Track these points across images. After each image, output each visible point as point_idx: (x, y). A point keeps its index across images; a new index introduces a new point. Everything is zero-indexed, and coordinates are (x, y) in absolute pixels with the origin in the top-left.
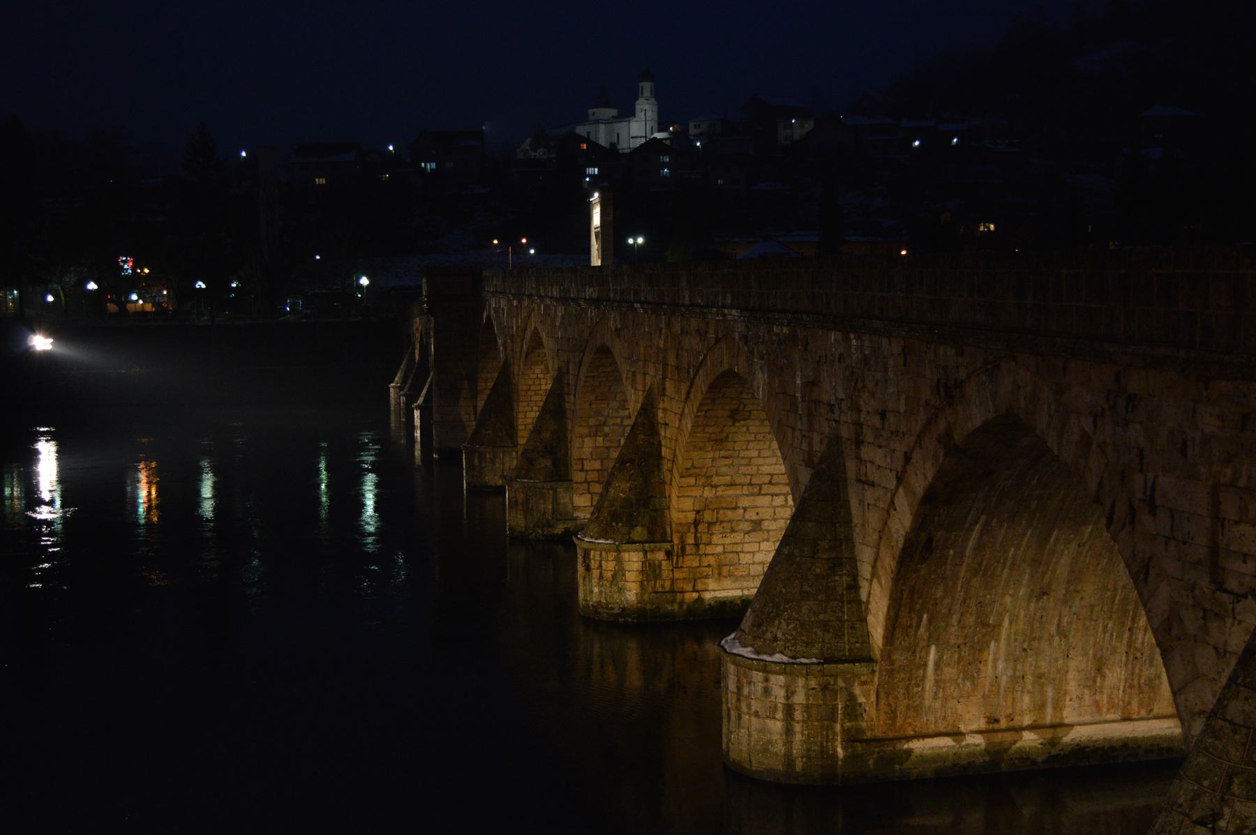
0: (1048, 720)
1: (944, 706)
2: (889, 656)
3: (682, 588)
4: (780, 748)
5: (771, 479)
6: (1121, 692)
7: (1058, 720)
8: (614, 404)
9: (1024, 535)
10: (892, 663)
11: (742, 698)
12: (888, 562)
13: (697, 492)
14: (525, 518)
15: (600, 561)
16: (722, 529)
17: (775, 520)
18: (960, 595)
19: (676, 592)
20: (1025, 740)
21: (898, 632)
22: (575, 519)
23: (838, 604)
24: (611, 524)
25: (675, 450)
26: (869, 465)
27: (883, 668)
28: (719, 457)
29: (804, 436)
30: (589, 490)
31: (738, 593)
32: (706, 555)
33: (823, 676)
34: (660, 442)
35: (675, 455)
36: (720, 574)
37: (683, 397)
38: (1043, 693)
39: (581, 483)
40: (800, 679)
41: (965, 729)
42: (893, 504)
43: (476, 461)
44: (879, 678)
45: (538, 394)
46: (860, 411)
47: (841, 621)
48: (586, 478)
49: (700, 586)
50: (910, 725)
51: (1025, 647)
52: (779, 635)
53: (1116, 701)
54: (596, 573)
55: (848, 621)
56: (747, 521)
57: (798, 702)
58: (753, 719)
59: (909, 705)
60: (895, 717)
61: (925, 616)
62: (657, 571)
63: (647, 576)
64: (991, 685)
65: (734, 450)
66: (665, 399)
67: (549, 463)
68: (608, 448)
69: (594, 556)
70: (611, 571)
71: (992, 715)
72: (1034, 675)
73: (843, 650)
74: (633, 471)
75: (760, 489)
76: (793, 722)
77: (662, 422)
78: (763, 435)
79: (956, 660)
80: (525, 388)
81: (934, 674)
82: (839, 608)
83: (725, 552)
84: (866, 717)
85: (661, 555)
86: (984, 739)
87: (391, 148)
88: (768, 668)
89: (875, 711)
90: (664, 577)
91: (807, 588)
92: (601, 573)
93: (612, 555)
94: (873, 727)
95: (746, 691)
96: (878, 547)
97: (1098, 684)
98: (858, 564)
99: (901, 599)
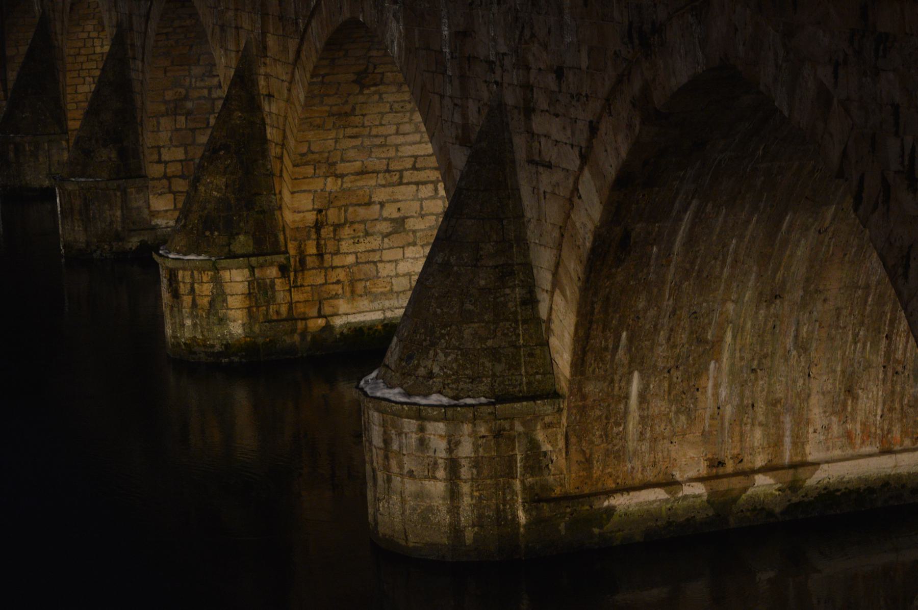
0: (787, 457)
1: (652, 449)
2: (580, 389)
3: (304, 313)
4: (444, 518)
5: (415, 162)
6: (878, 418)
7: (798, 459)
8: (196, 71)
9: (748, 222)
10: (584, 397)
11: (390, 454)
12: (573, 267)
13: (318, 184)
14: (86, 230)
15: (192, 285)
16: (352, 232)
17: (422, 216)
18: (668, 303)
19: (296, 320)
20: (758, 486)
21: (590, 358)
22: (154, 228)
23: (511, 325)
24: (204, 233)
25: (284, 130)
26: (543, 140)
27: (572, 405)
28: (344, 137)
29: (456, 105)
30: (170, 187)
31: (377, 316)
32: (333, 268)
33: (496, 419)
34: (263, 120)
35: (285, 137)
36: (353, 292)
37: (292, 56)
38: (778, 422)
39: (159, 179)
40: (465, 426)
41: (681, 477)
42: (578, 190)
43: (12, 155)
44: (567, 418)
45: (92, 60)
46: (528, 69)
47: (515, 346)
48: (165, 173)
49: (327, 310)
50: (610, 476)
51: (754, 367)
52: (436, 370)
53: (873, 430)
54: (187, 300)
55: (524, 346)
56: (385, 219)
57: (464, 456)
58: (406, 480)
59: (608, 450)
60: (591, 468)
61: (624, 334)
62: (270, 293)
63: (257, 300)
64: (712, 418)
65: (363, 126)
66: (268, 61)
67: (114, 155)
68: (193, 130)
70: (208, 296)
71: (715, 457)
72: (766, 403)
73: (520, 385)
75: (401, 177)
76: (458, 482)
77: (265, 93)
78: (402, 104)
79: (666, 389)
80: (72, 52)
81: (639, 409)
82: (512, 330)
83: (357, 263)
85: (273, 272)
86: (706, 489)
88: (424, 413)
89: (564, 461)
90: (279, 300)
91: (469, 306)
92: (194, 300)
95: (395, 446)
96: (559, 247)
97: (849, 409)
98: (535, 271)
99: (592, 313)
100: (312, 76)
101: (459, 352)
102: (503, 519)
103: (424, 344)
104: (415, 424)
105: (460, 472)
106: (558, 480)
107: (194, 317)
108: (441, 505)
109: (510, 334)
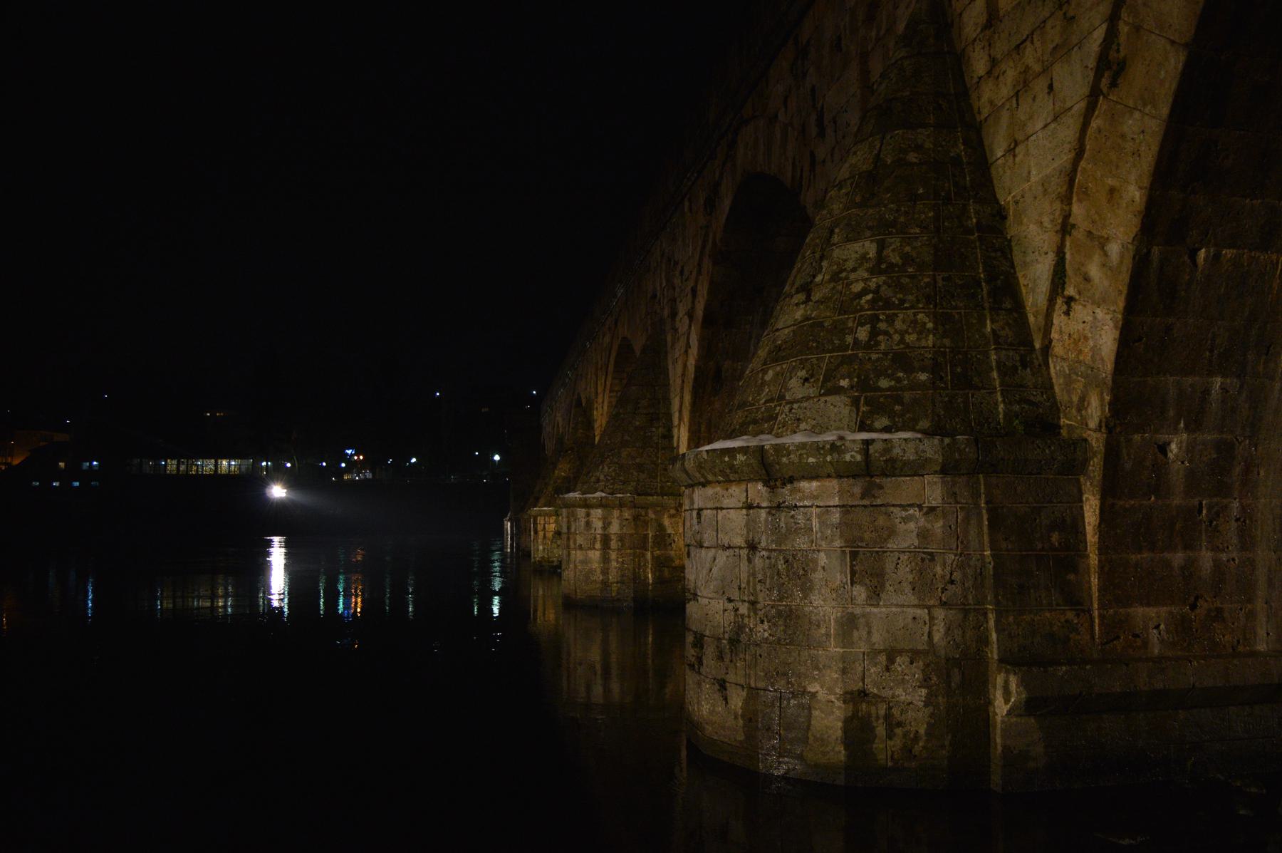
12: (688, 398)
33: (635, 507)
40: (615, 511)
52: (602, 477)
54: (541, 534)
55: (661, 464)
58: (578, 552)
87: (534, 392)
91: (627, 437)
92: (545, 535)
93: (552, 519)
95: (573, 530)
100: (610, 392)
102: (637, 579)
107: (544, 544)
108: (595, 565)
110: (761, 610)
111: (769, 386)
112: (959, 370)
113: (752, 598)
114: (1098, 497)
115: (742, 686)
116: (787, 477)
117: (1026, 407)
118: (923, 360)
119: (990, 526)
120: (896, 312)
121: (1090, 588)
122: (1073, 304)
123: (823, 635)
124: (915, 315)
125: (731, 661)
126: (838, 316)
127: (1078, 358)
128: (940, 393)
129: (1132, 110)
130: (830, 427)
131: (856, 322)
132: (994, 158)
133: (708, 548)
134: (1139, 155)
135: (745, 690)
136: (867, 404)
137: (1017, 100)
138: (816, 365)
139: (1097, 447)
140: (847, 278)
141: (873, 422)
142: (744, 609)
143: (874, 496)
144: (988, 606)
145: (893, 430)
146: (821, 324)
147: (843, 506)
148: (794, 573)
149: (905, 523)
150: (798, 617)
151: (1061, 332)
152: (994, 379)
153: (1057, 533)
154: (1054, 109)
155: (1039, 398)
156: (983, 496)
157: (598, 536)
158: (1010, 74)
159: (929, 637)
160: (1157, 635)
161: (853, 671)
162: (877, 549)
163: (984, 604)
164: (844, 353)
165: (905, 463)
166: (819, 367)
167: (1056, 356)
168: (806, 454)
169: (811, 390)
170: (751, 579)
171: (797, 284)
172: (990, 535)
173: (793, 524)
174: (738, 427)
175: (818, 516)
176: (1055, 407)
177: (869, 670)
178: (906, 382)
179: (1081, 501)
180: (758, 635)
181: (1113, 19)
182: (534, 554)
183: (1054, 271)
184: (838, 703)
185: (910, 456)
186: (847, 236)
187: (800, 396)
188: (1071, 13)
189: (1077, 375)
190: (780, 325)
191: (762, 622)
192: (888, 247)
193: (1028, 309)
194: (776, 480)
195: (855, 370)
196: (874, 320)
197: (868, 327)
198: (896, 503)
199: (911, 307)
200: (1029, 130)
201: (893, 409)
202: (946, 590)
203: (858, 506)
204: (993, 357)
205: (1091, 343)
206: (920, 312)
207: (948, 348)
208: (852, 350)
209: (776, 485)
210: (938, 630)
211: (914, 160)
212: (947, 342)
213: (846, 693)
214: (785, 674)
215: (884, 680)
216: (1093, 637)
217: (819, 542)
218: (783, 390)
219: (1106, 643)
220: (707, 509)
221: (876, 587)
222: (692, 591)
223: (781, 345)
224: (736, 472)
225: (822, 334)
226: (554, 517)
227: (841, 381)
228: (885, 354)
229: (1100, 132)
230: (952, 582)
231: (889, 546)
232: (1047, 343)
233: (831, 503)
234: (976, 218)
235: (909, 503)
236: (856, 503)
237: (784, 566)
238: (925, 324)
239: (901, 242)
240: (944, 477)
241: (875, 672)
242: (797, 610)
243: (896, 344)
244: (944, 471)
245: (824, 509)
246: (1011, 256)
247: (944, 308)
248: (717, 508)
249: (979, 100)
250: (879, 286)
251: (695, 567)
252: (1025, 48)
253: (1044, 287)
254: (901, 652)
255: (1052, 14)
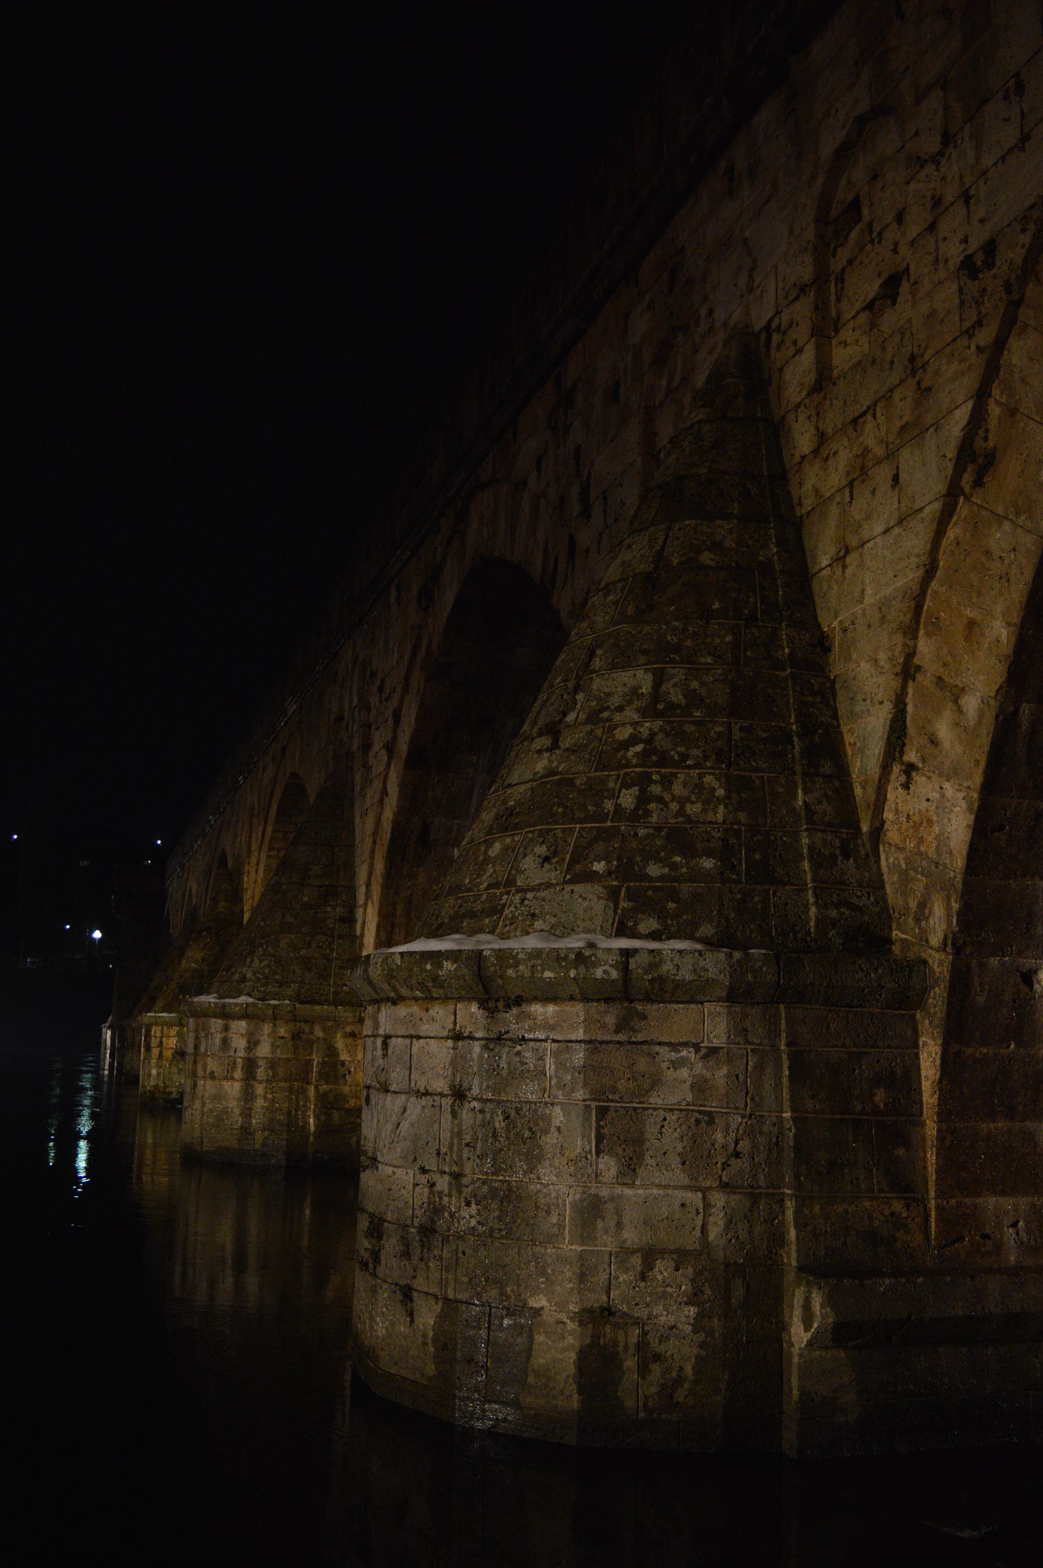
4: (237, 1120)
12: (380, 866)
15: (161, 1038)
23: (327, 940)
33: (295, 1020)
34: (243, 909)
40: (266, 1025)
47: (327, 959)
52: (249, 975)
54: (155, 1051)
58: (208, 1082)
69: (155, 1032)
70: (172, 1048)
73: (327, 994)
74: (209, 940)
82: (327, 943)
84: (350, 1080)
91: (289, 919)
92: (161, 1052)
93: (174, 1031)
94: (358, 1094)
95: (202, 1049)
100: (269, 850)
101: (273, 959)
103: (244, 953)
104: (220, 1023)
105: (256, 1072)
106: (354, 1091)
107: (159, 1067)
108: (233, 1105)
109: (325, 947)
110: (467, 1187)
111: (494, 865)
112: (757, 857)
113: (455, 1169)
114: (939, 1042)
115: (436, 1297)
116: (513, 997)
117: (847, 912)
118: (708, 840)
119: (792, 1076)
120: (675, 771)
121: (925, 1168)
122: (914, 774)
123: (554, 1225)
124: (701, 776)
125: (422, 1260)
126: (595, 771)
127: (918, 848)
128: (730, 887)
129: (1001, 518)
130: (576, 929)
131: (620, 781)
132: (817, 568)
133: (395, 1092)
134: (1008, 581)
135: (440, 1303)
136: (629, 897)
137: (851, 492)
138: (561, 838)
139: (940, 973)
140: (609, 719)
141: (636, 924)
142: (443, 1183)
143: (634, 1030)
144: (786, 1190)
145: (664, 937)
146: (570, 782)
147: (590, 1042)
148: (516, 1135)
149: (675, 1069)
150: (519, 1198)
151: (897, 812)
152: (805, 871)
153: (882, 1090)
154: (899, 509)
155: (864, 900)
156: (784, 1035)
157: (239, 1060)
158: (844, 457)
159: (702, 1232)
160: (1014, 1236)
161: (594, 1279)
162: (634, 1105)
163: (779, 1188)
164: (603, 825)
165: (678, 985)
166: (566, 842)
167: (890, 844)
168: (541, 965)
169: (553, 875)
170: (455, 1141)
171: (541, 723)
172: (792, 1090)
173: (518, 1065)
174: (447, 920)
175: (555, 1054)
176: (885, 914)
177: (617, 1278)
178: (684, 870)
179: (917, 1046)
180: (462, 1222)
181: (981, 396)
182: (143, 1081)
183: (891, 727)
184: (571, 1326)
185: (686, 974)
186: (613, 661)
187: (537, 882)
188: (926, 383)
189: (916, 871)
190: (514, 779)
191: (468, 1204)
192: (668, 680)
193: (854, 776)
194: (497, 1001)
195: (615, 849)
196: (644, 780)
197: (635, 790)
198: (663, 1040)
199: (697, 766)
200: (865, 534)
201: (665, 907)
202: (729, 1165)
203: (610, 1042)
204: (805, 841)
205: (936, 829)
206: (708, 773)
207: (745, 825)
208: (612, 821)
209: (497, 1007)
210: (716, 1223)
211: (711, 563)
212: (742, 816)
213: (584, 1310)
214: (497, 1282)
215: (638, 1292)
216: (927, 1237)
217: (554, 1091)
218: (514, 872)
219: (946, 1246)
220: (397, 1036)
221: (631, 1158)
222: (370, 1154)
223: (513, 808)
224: (441, 987)
225: (571, 796)
226: (177, 1028)
227: (595, 863)
228: (658, 829)
229: (958, 544)
230: (737, 1155)
231: (651, 1100)
232: (878, 824)
233: (573, 1037)
234: (788, 647)
235: (681, 1041)
236: (608, 1038)
237: (503, 1124)
238: (714, 789)
239: (686, 674)
240: (733, 1006)
241: (625, 1281)
242: (518, 1188)
243: (673, 816)
244: (731, 998)
245: (563, 1045)
246: (835, 703)
247: (740, 770)
248: (411, 1037)
249: (800, 488)
250: (653, 734)
251: (375, 1120)
252: (865, 421)
253: (876, 749)
254: (662, 1252)
255: (902, 381)
